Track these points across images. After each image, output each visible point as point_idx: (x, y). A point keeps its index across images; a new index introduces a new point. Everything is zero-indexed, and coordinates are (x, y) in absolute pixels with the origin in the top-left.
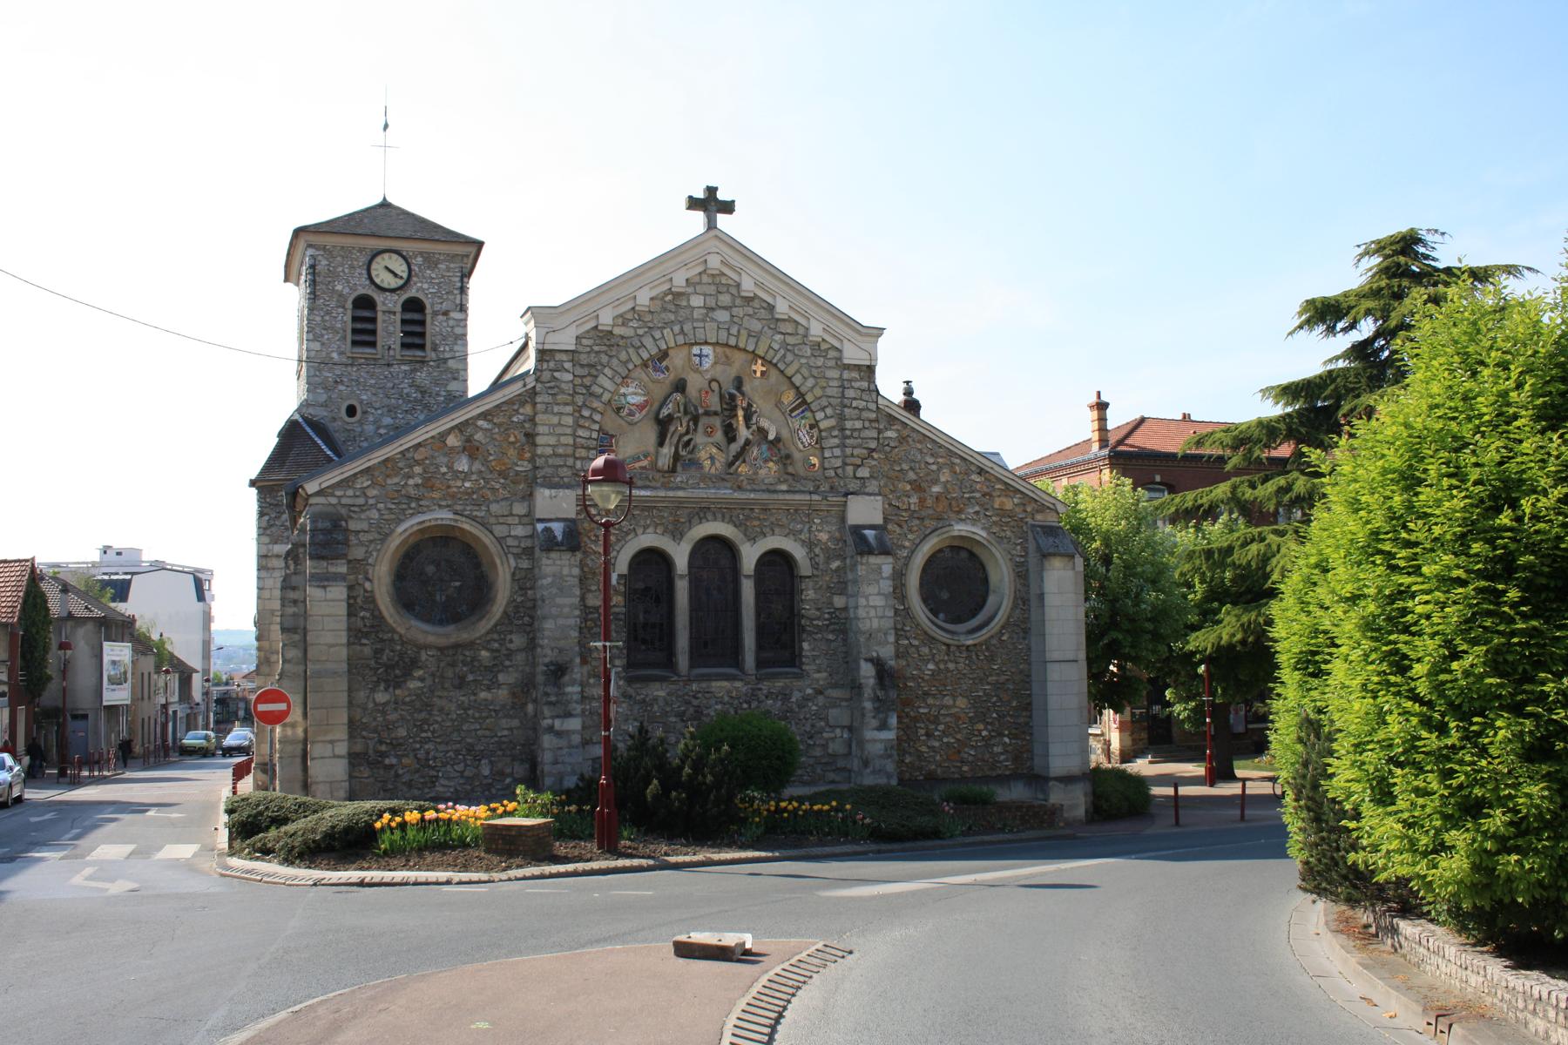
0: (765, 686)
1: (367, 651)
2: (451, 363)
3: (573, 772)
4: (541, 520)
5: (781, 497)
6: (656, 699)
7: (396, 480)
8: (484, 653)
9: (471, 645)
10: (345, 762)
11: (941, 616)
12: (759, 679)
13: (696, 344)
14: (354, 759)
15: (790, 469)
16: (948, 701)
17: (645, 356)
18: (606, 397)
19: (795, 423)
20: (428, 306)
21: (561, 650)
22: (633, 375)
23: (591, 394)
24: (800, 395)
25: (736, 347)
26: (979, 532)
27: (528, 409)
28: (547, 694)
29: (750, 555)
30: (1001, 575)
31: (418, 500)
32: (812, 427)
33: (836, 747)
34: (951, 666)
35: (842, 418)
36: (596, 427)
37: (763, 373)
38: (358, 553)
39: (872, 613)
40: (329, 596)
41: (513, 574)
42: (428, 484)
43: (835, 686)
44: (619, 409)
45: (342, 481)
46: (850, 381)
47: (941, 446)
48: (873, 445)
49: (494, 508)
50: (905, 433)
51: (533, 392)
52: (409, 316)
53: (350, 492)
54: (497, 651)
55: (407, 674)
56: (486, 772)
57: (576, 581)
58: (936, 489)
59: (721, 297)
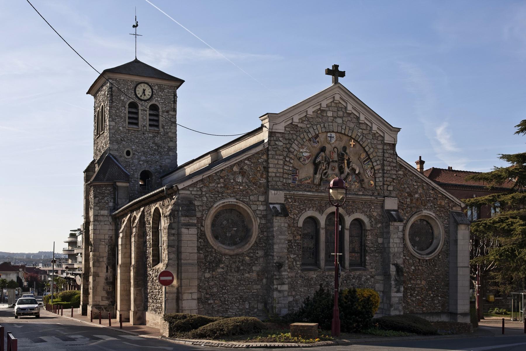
0: (352, 274)
3: (285, 307)
4: (272, 204)
5: (360, 197)
6: (312, 278)
8: (247, 258)
10: (196, 302)
11: (416, 247)
13: (330, 132)
15: (364, 186)
17: (310, 136)
18: (295, 153)
20: (160, 108)
21: (281, 257)
22: (306, 144)
23: (289, 151)
24: (368, 155)
25: (344, 134)
26: (432, 214)
28: (276, 275)
29: (348, 220)
30: (440, 231)
31: (222, 193)
32: (371, 168)
34: (420, 268)
35: (383, 165)
36: (291, 165)
40: (190, 232)
41: (259, 226)
42: (226, 187)
45: (192, 184)
46: (387, 150)
47: (419, 178)
48: (394, 177)
49: (252, 198)
50: (407, 172)
51: (268, 150)
53: (195, 189)
54: (252, 257)
55: (217, 266)
56: (247, 307)
58: (417, 196)
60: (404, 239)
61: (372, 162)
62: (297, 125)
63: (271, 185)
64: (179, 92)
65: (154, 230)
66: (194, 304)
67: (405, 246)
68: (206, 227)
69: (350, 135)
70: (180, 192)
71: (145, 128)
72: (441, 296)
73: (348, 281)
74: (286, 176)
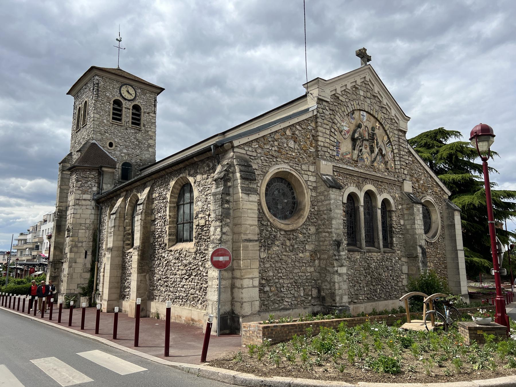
2: (150, 133)
4: (324, 175)
7: (268, 147)
17: (349, 111)
20: (142, 109)
23: (333, 123)
28: (335, 255)
43: (403, 256)
44: (342, 131)
47: (422, 166)
49: (304, 167)
51: (316, 117)
53: (250, 149)
56: (302, 295)
61: (392, 146)
62: (338, 98)
63: (321, 155)
64: (159, 98)
65: (172, 205)
70: (236, 150)
71: (128, 124)
73: (384, 263)
74: (332, 147)
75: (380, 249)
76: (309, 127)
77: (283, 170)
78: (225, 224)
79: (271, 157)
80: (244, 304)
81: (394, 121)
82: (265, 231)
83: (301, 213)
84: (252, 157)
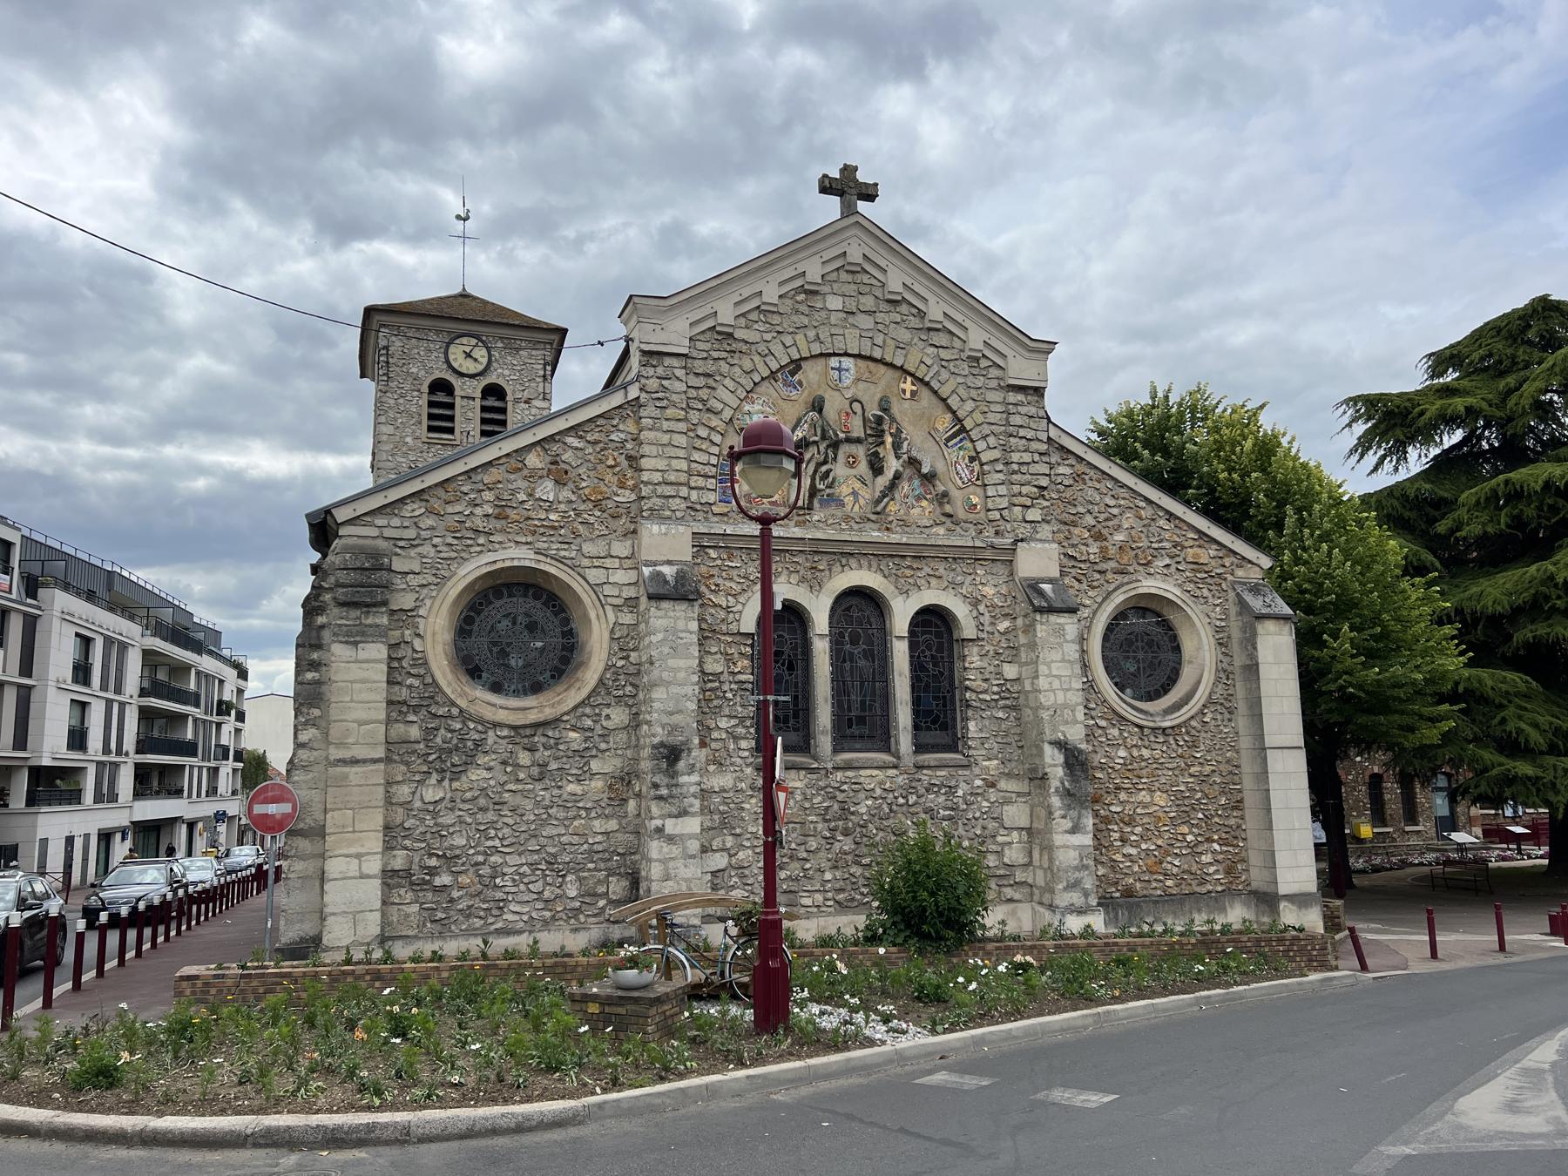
1: (414, 732)
7: (458, 508)
8: (573, 735)
9: (554, 722)
12: (919, 767)
13: (835, 355)
14: (390, 878)
15: (948, 509)
16: (1144, 796)
17: (775, 366)
18: (727, 414)
19: (952, 454)
22: (758, 389)
25: (881, 361)
27: (630, 426)
28: (656, 786)
29: (902, 614)
32: (972, 459)
33: (1014, 855)
34: (1146, 753)
37: (913, 393)
38: (407, 601)
39: (1056, 684)
40: (362, 655)
41: (612, 631)
43: (1009, 775)
47: (1124, 486)
48: (1044, 482)
49: (588, 548)
52: (491, 402)
53: (396, 522)
55: (470, 760)
57: (695, 638)
58: (1119, 537)
59: (863, 299)
60: (1085, 666)
62: (731, 335)
63: (650, 509)
66: (372, 891)
67: (1090, 686)
68: (429, 638)
69: (898, 362)
71: (471, 439)
72: (1223, 842)
74: (700, 482)
75: (898, 758)
76: (613, 437)
77: (508, 564)
78: (306, 723)
79: (470, 534)
80: (330, 920)
81: (984, 363)
82: (442, 731)
83: (579, 674)
84: (401, 544)
